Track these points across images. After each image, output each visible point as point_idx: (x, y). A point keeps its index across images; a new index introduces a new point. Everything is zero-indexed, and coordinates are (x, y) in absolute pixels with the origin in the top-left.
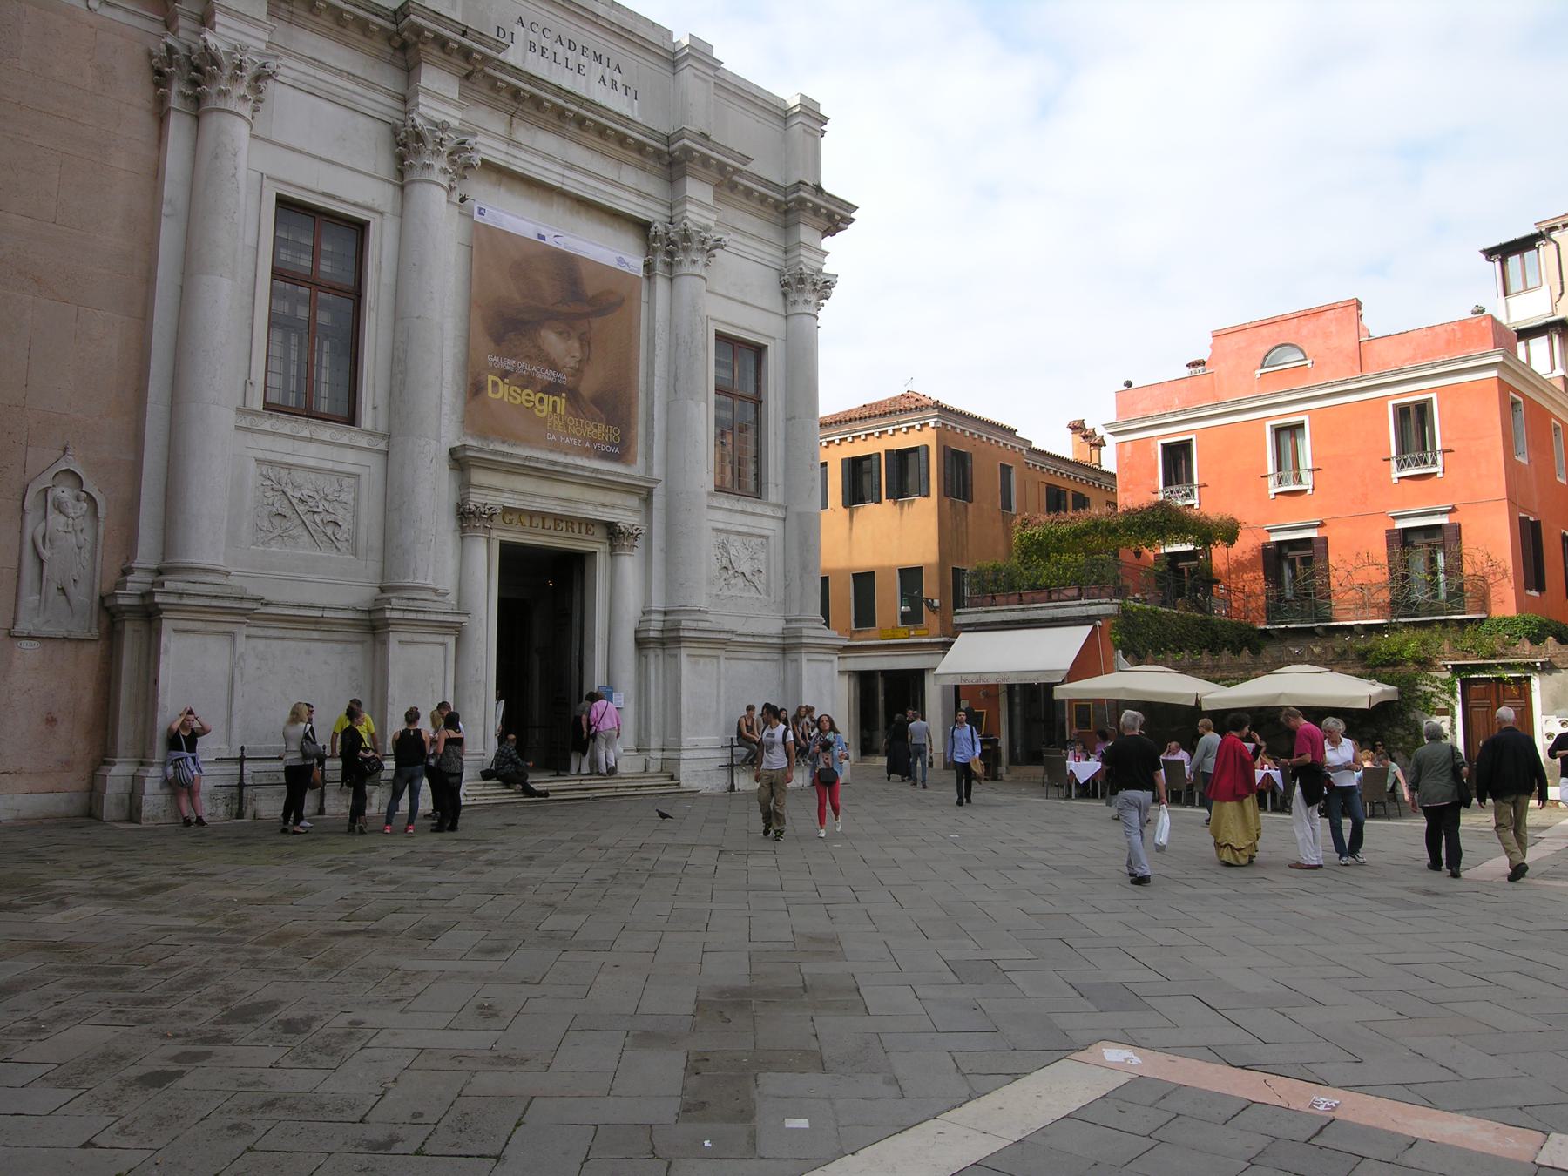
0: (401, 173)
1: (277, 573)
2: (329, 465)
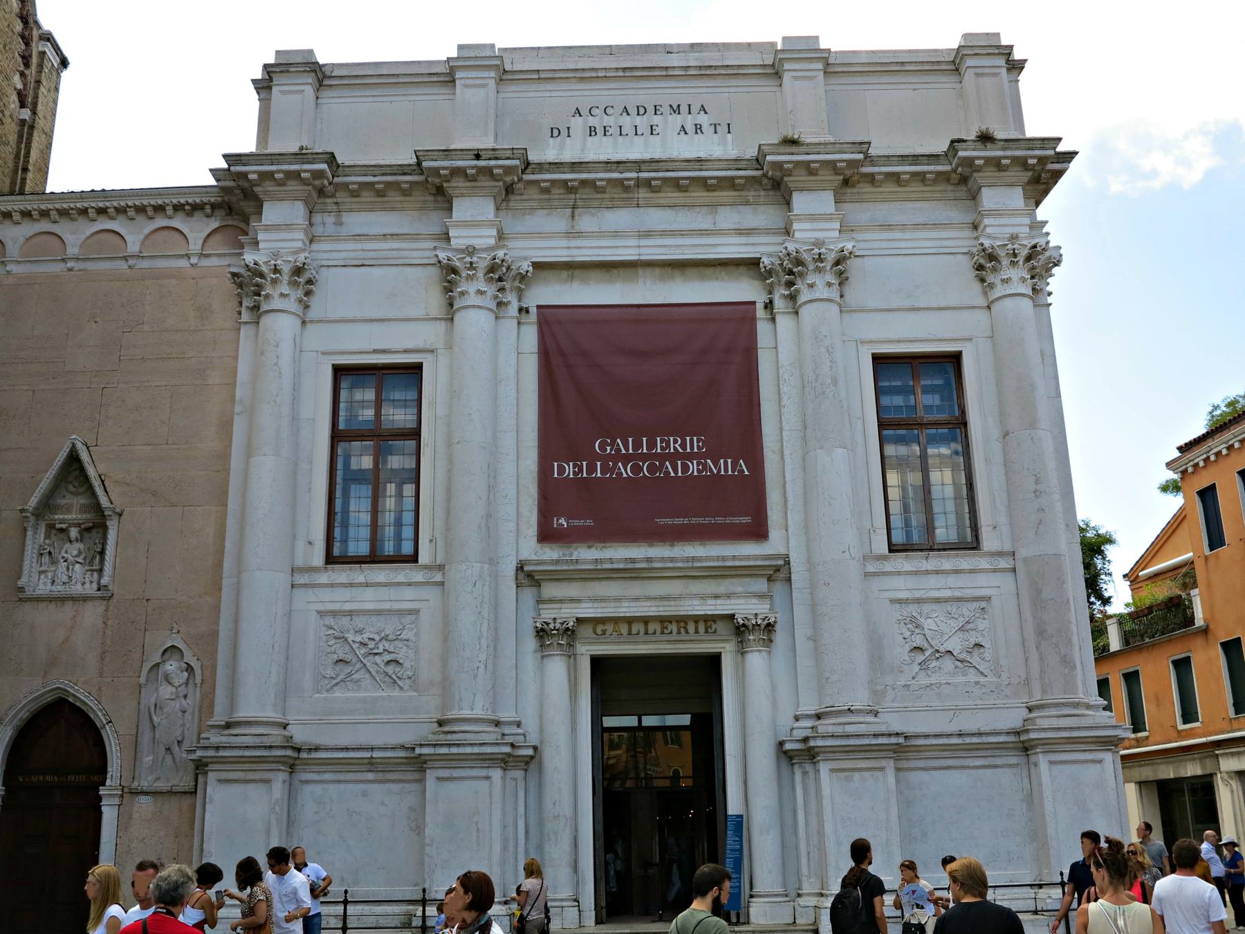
1: (337, 717)
2: (387, 606)
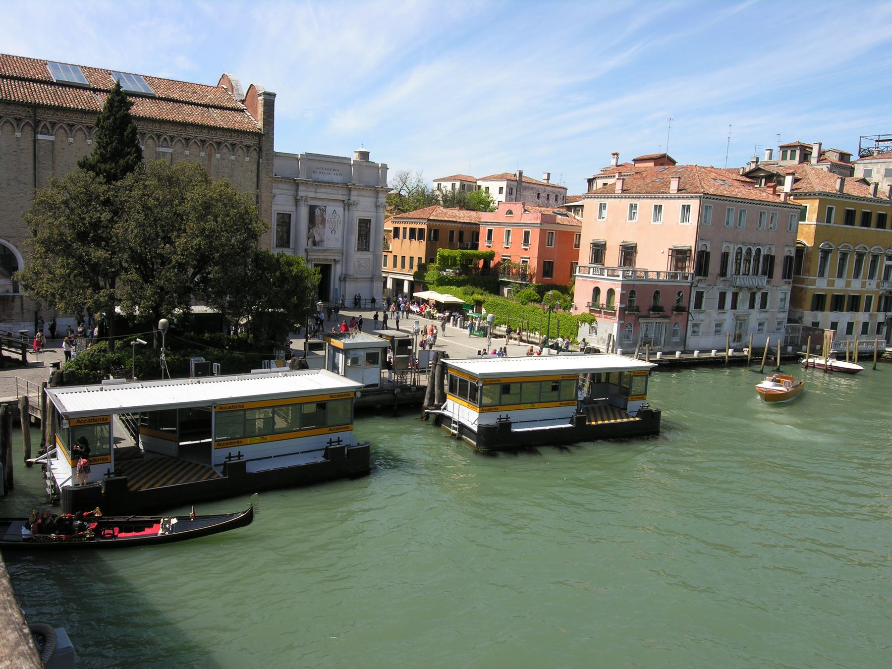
0: (296, 204)
